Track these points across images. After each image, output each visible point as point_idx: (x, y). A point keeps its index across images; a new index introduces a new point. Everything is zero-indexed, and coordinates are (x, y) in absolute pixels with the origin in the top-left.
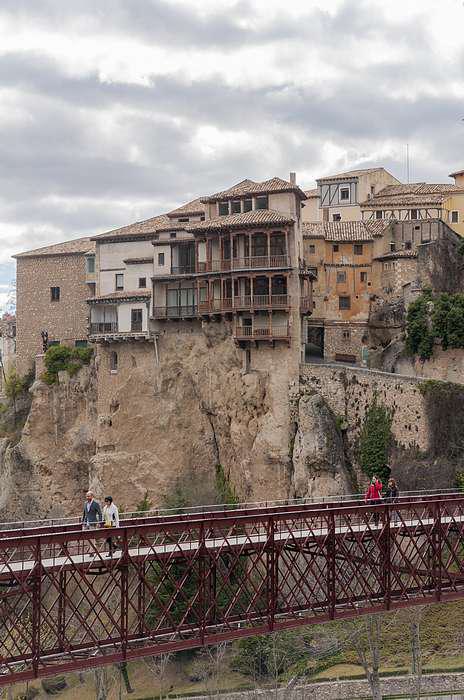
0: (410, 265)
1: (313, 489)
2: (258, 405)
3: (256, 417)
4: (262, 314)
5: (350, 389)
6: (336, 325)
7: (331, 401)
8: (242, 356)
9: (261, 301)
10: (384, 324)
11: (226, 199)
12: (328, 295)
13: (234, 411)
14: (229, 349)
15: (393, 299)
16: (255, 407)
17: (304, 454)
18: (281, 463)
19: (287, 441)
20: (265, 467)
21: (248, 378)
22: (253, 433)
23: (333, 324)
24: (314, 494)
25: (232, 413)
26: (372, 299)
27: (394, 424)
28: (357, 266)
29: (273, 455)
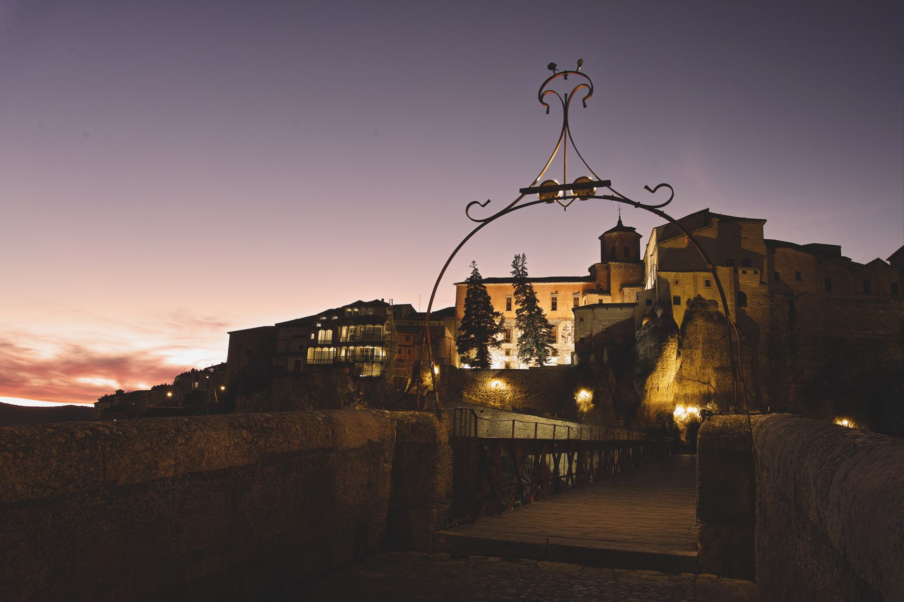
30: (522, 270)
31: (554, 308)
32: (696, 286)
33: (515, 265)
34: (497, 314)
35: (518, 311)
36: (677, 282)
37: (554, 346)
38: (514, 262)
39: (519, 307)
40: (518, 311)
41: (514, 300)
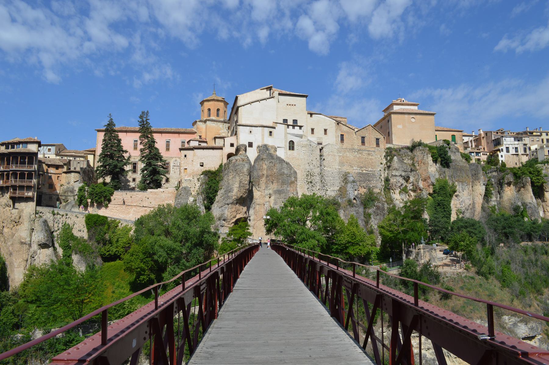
0: (77, 175)
1: (40, 254)
2: (17, 222)
3: (15, 226)
4: (22, 188)
5: (56, 216)
6: (47, 194)
7: (48, 221)
8: (11, 203)
9: (22, 182)
10: (66, 194)
11: (9, 143)
12: (45, 183)
13: (6, 224)
14: (5, 200)
15: (70, 186)
16: (16, 223)
17: (37, 240)
18: (26, 244)
19: (29, 235)
20: (19, 245)
21: (14, 211)
22: (14, 233)
23: (46, 194)
24: (40, 256)
25: (4, 225)
26: (61, 186)
27: (73, 230)
28: (56, 174)
29: (23, 241)
30: (146, 121)
31: (168, 149)
32: (263, 135)
33: (141, 117)
34: (126, 152)
35: (142, 150)
36: (251, 132)
37: (167, 175)
38: (141, 115)
39: (143, 147)
40: (142, 150)
41: (139, 142)
